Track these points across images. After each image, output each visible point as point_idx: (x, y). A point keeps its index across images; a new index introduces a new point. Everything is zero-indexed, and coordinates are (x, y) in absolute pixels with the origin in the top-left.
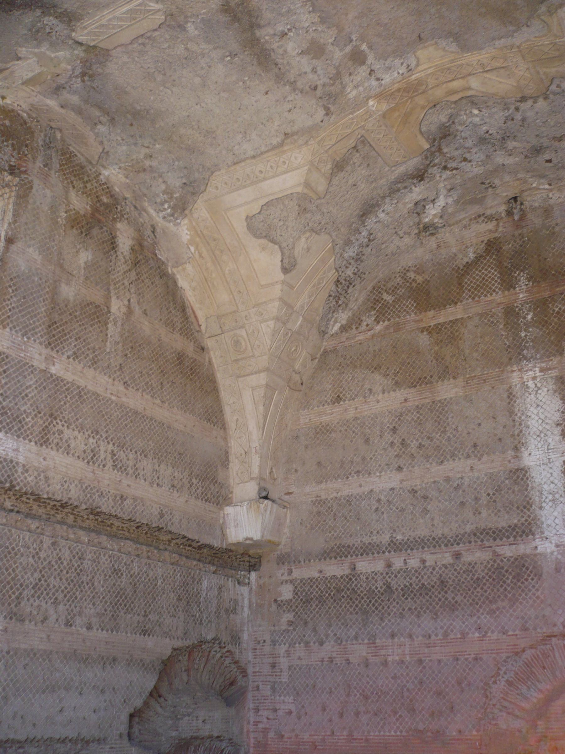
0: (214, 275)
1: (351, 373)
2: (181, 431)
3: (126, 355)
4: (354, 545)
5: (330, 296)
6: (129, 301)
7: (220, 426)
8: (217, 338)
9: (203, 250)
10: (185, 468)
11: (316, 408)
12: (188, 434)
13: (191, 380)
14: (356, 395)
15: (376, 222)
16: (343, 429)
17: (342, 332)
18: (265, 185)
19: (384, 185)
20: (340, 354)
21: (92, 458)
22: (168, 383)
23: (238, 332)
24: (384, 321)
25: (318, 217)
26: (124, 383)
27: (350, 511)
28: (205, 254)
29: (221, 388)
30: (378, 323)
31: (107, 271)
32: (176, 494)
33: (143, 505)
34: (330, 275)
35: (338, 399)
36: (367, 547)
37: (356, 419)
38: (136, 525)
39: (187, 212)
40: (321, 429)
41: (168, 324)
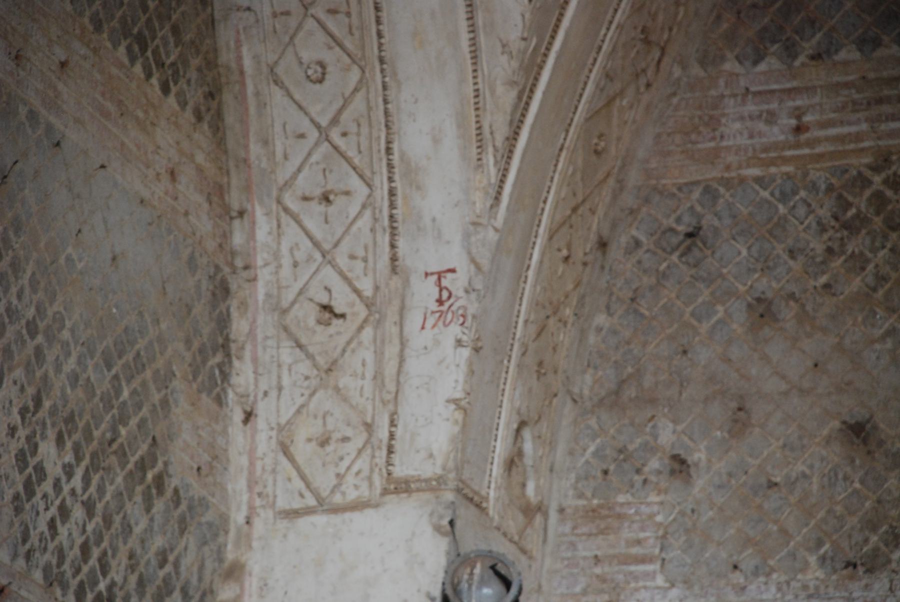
7: (195, 96)
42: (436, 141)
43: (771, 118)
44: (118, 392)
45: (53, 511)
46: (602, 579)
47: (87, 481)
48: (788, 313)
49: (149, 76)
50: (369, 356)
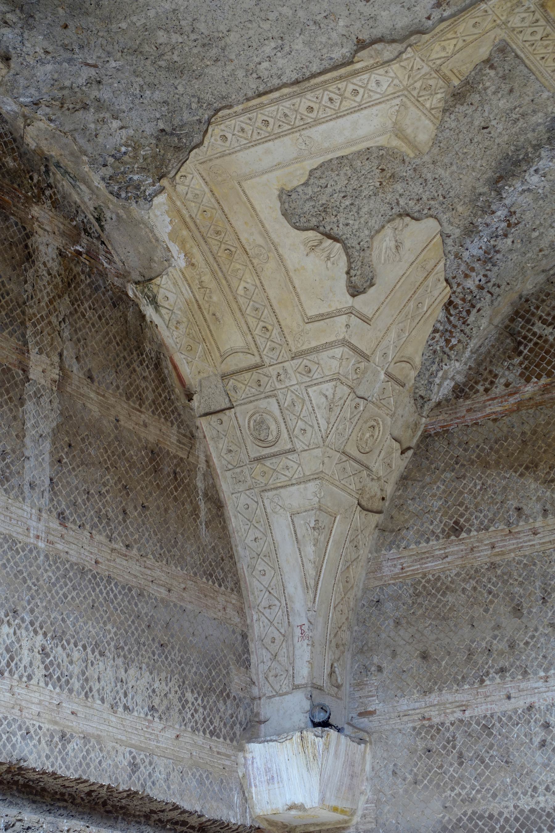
0: (215, 299)
1: (480, 478)
2: (162, 600)
3: (59, 461)
4: (501, 814)
5: (436, 331)
6: (61, 355)
7: (231, 585)
8: (220, 415)
9: (195, 250)
10: (172, 671)
11: (413, 546)
12: (175, 605)
13: (175, 499)
14: (492, 521)
15: (524, 191)
16: (468, 587)
17: (457, 397)
18: (317, 133)
19: (539, 125)
20: (456, 441)
21: (8, 665)
22: (135, 508)
23: (263, 404)
24: (539, 377)
25: (416, 189)
26: (59, 515)
27: (491, 747)
28: (198, 258)
29: (230, 510)
30: (528, 380)
31: (21, 301)
32: (158, 725)
33: (101, 750)
34: (436, 293)
35: (456, 529)
36: (527, 818)
37: (493, 566)
38: (87, 790)
39: (165, 182)
40: (424, 586)
41: (132, 395)
42: (296, 588)
43: (395, 566)
44: (211, 674)
45: (192, 711)
46: (362, 703)
47: (203, 700)
48: (404, 621)
49: (214, 583)
50: (285, 650)
